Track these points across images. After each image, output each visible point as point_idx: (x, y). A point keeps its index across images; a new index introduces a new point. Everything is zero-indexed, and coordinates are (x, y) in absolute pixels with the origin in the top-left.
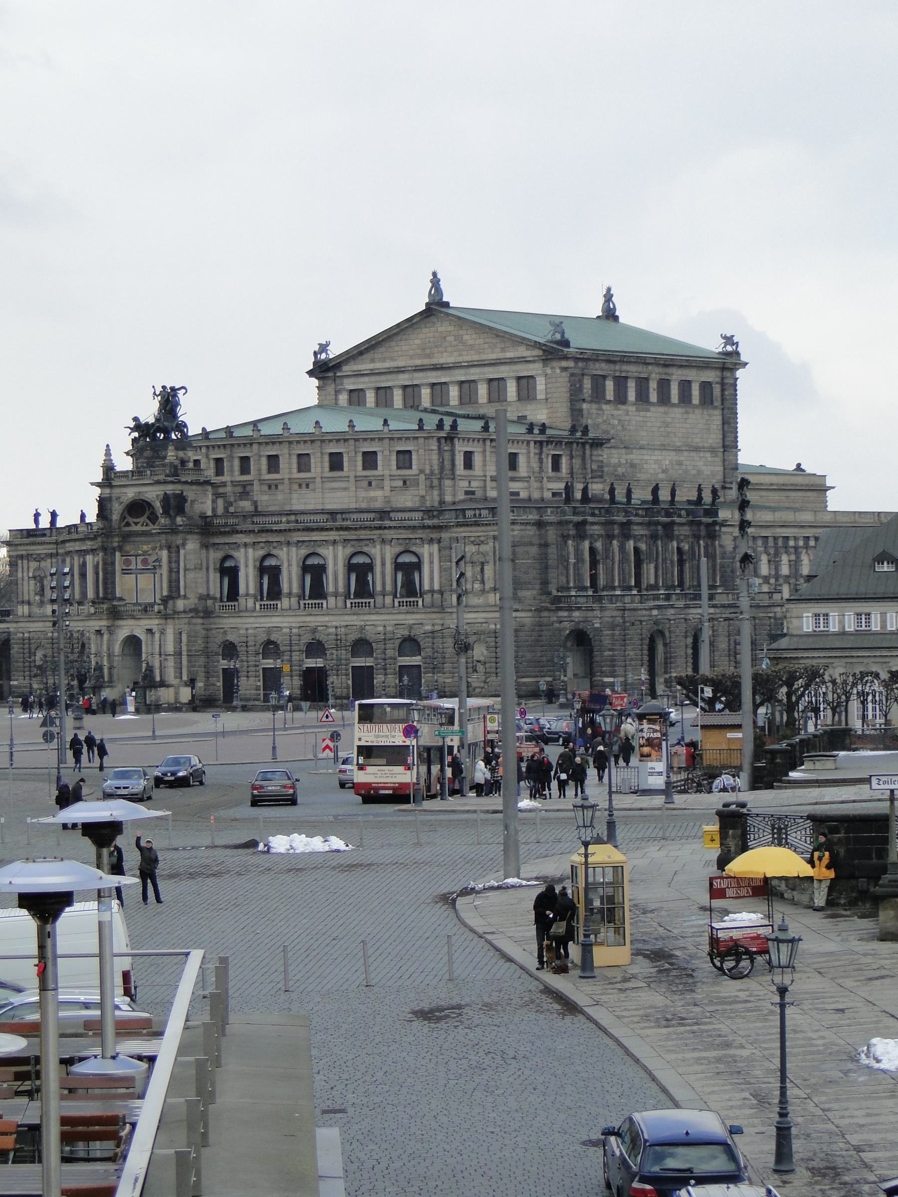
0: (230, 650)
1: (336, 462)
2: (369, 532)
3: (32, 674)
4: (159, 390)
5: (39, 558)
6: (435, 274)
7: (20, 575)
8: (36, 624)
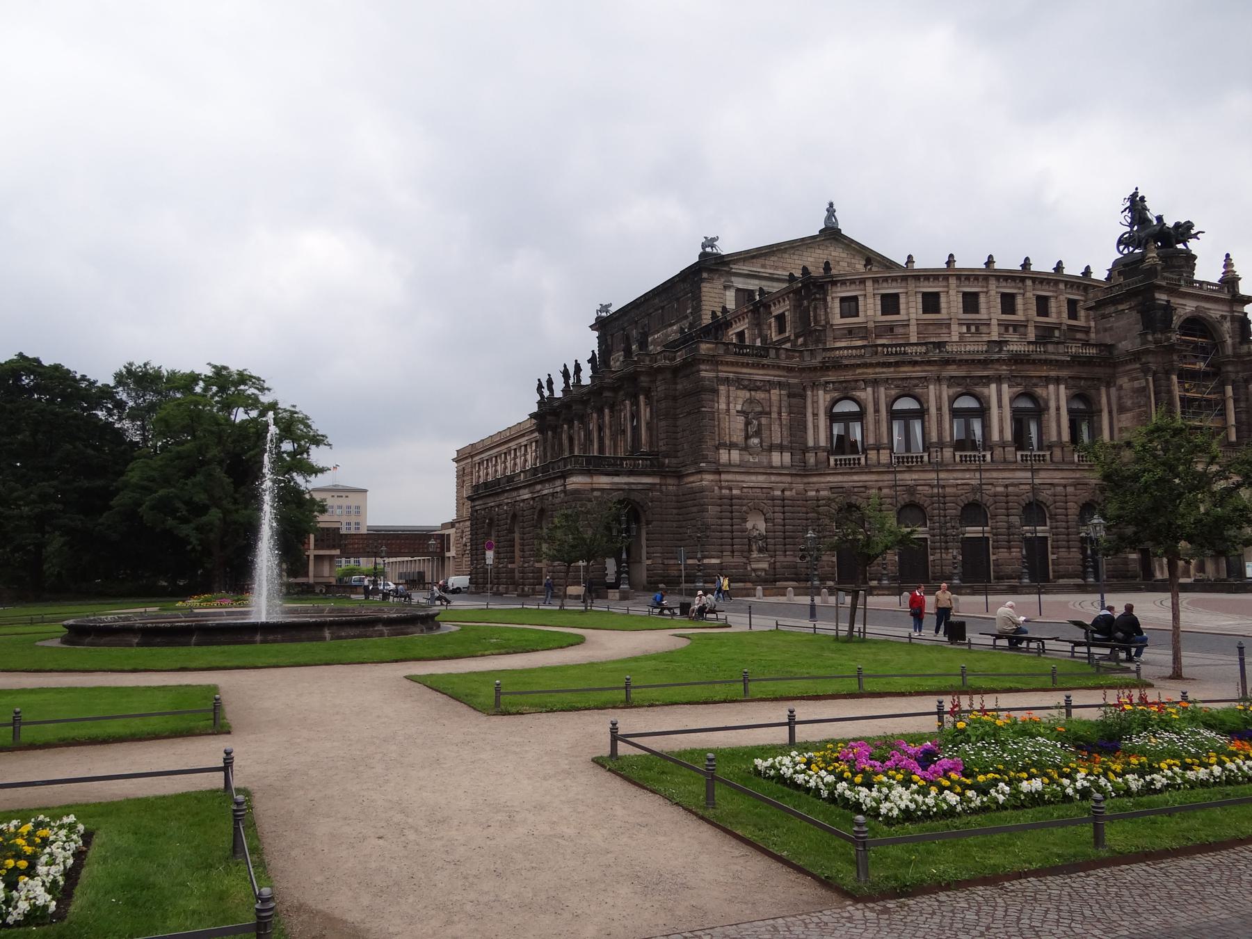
5: (753, 387)
6: (831, 205)
8: (753, 478)
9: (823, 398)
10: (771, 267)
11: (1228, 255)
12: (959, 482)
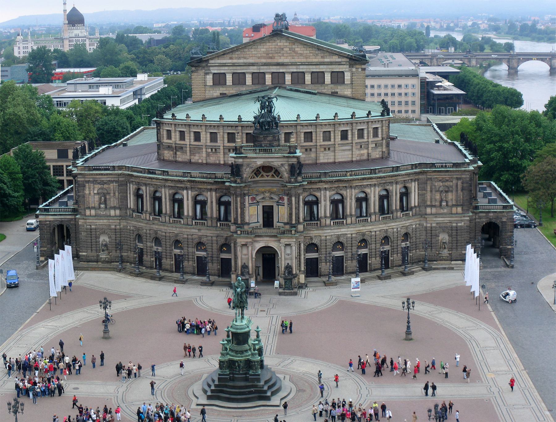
1: (344, 135)
8: (102, 221)
9: (132, 188)
10: (236, 58)
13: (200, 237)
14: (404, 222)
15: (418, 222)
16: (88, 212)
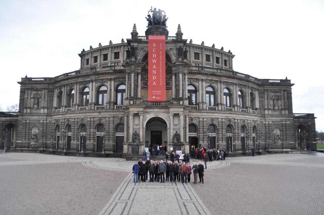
0: (193, 127)
2: (245, 82)
3: (30, 138)
4: (153, 9)
5: (37, 90)
7: (26, 96)
8: (34, 117)
9: (56, 92)
11: (179, 25)
12: (78, 117)
13: (100, 119)
14: (253, 117)
15: (260, 120)
16: (25, 111)
